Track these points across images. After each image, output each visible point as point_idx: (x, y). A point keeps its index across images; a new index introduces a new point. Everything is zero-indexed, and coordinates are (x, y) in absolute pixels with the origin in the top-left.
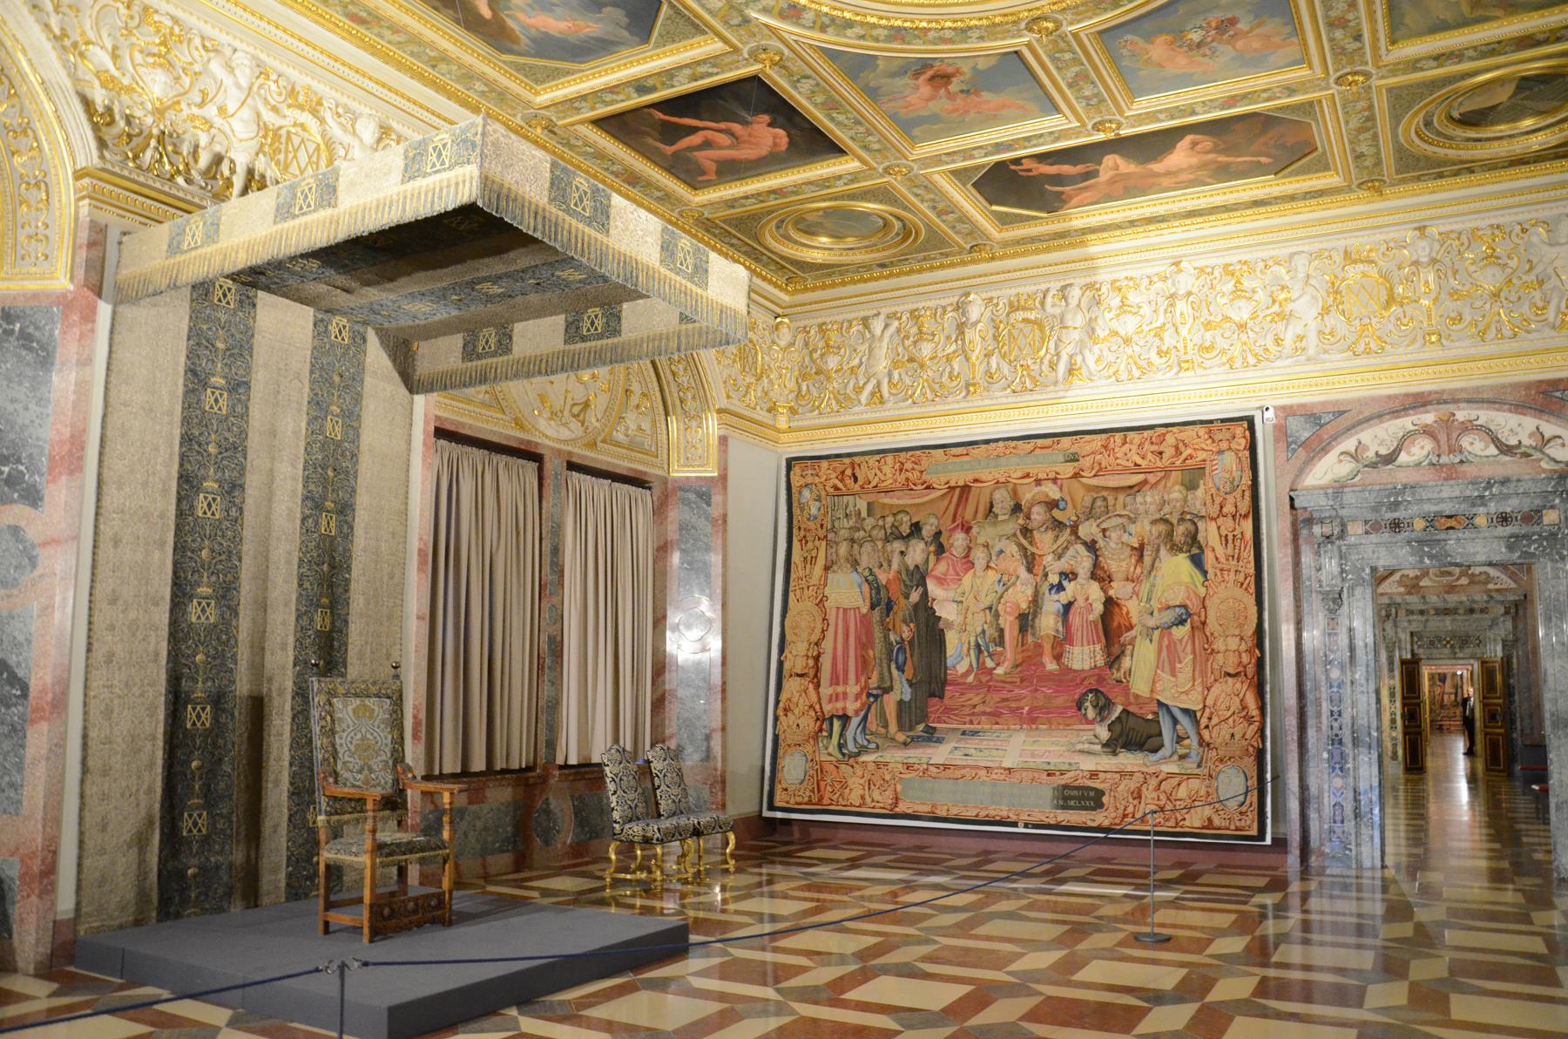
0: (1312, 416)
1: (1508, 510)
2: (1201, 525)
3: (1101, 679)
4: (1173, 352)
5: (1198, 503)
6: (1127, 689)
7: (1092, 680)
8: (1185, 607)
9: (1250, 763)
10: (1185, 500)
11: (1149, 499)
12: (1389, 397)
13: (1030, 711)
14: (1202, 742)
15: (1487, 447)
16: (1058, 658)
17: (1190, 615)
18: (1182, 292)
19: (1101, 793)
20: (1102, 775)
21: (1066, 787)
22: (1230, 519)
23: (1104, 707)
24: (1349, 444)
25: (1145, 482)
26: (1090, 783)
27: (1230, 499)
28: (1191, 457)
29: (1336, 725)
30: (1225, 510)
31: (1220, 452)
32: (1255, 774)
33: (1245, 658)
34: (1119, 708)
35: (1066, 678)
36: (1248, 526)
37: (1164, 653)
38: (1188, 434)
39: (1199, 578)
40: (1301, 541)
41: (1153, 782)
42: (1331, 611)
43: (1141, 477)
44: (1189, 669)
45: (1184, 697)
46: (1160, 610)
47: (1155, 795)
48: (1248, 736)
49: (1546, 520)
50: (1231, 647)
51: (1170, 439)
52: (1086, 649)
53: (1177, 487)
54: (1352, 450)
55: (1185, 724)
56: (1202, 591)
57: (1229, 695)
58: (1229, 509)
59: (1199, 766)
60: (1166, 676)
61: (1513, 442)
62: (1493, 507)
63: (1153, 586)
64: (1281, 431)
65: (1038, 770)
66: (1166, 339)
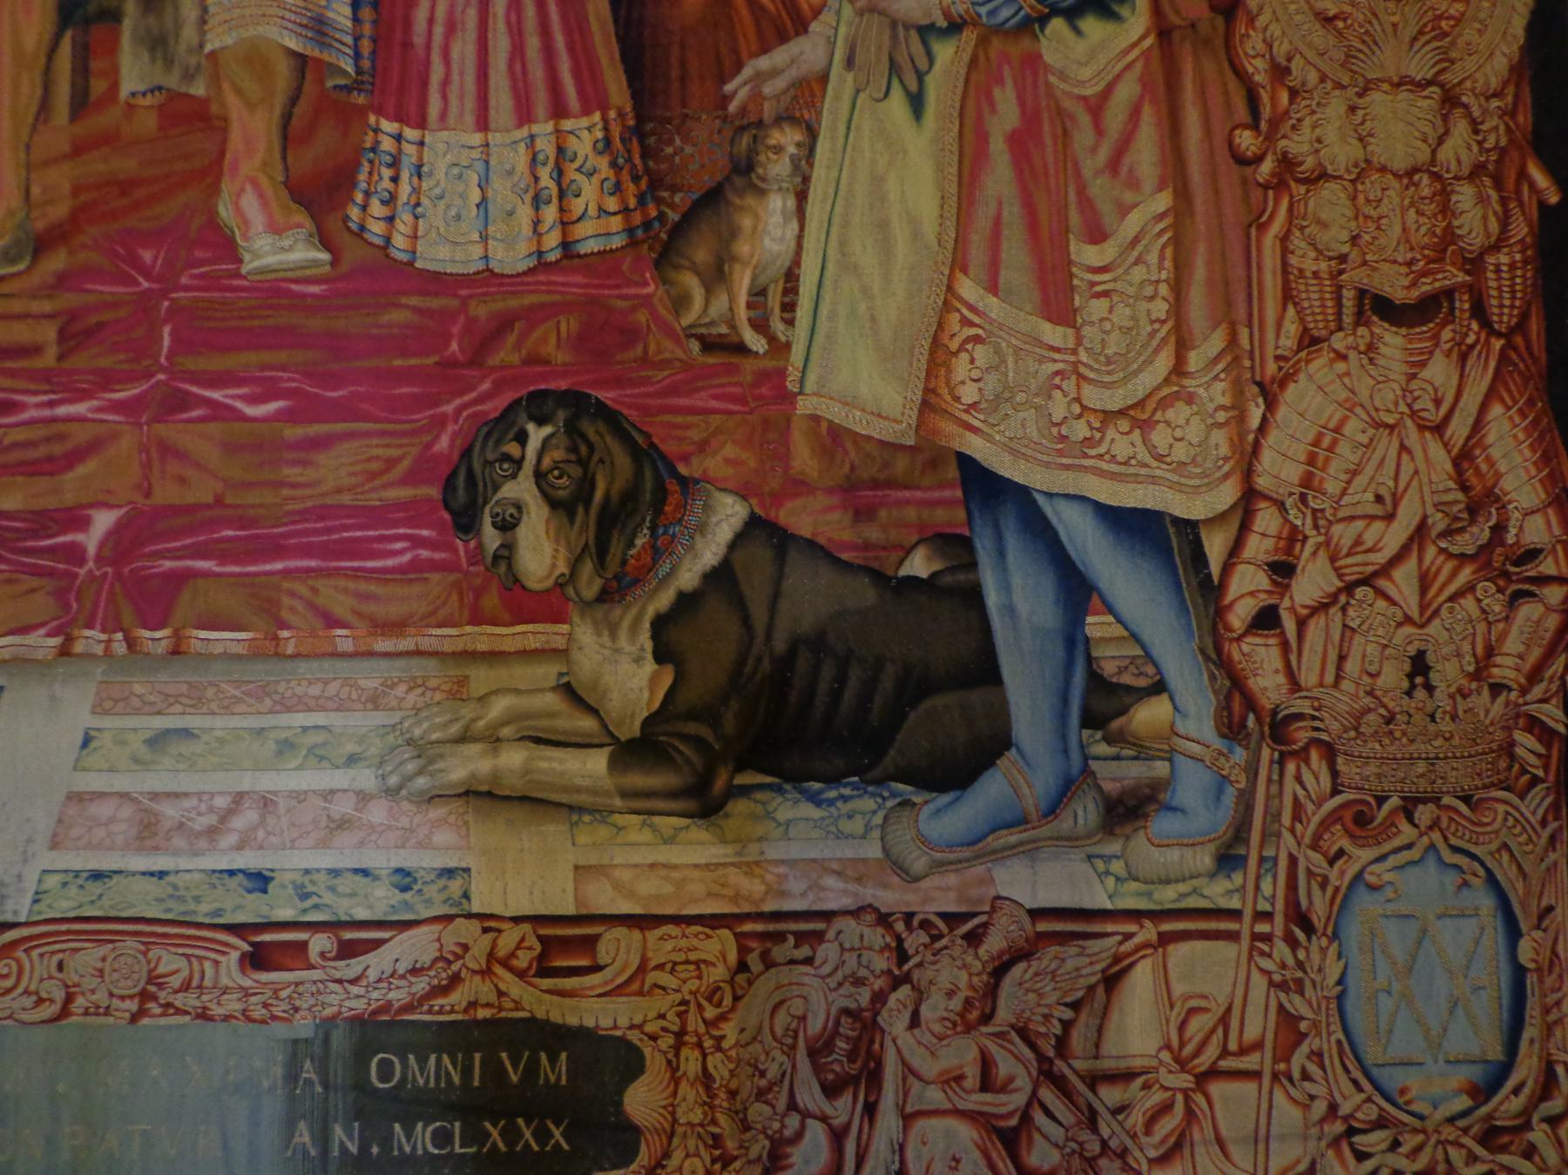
3: (606, 335)
6: (775, 390)
7: (553, 341)
13: (123, 543)
16: (320, 194)
19: (620, 1059)
20: (619, 949)
21: (372, 1031)
23: (621, 508)
26: (533, 1000)
33: (1473, 216)
34: (727, 516)
35: (385, 328)
37: (1000, 178)
41: (951, 975)
44: (1153, 269)
45: (1121, 442)
47: (962, 1054)
48: (1506, 669)
52: (510, 149)
59: (1228, 860)
60: (1009, 312)
65: (183, 930)
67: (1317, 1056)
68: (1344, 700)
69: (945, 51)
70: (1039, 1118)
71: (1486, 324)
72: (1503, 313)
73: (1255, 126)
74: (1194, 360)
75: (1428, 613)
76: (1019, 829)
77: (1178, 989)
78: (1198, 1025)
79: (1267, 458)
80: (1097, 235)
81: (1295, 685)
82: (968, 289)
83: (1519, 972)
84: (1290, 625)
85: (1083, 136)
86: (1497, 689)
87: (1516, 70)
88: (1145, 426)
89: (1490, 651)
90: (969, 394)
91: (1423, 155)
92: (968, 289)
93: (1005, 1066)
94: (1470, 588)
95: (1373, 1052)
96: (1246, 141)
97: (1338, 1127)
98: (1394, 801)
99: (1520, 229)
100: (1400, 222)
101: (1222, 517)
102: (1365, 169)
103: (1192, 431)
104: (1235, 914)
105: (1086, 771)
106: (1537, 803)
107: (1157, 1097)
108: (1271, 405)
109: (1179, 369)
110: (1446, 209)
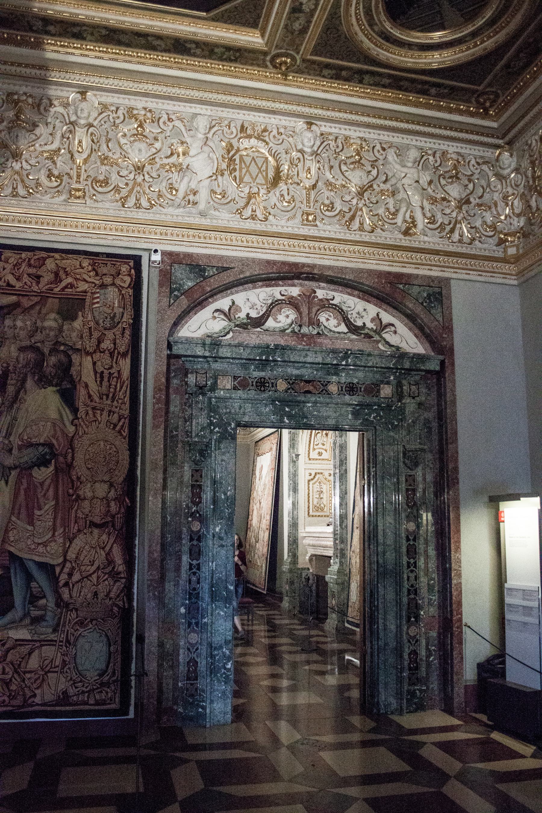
0: (197, 267)
1: (355, 381)
2: (75, 358)
4: (65, 178)
5: (74, 334)
8: (50, 446)
9: (112, 625)
10: (60, 330)
11: (19, 323)
12: (268, 262)
14: (60, 602)
15: (339, 325)
17: (54, 455)
18: (82, 122)
22: (107, 355)
24: (224, 303)
25: (17, 305)
27: (110, 335)
28: (71, 286)
29: (194, 579)
30: (103, 346)
31: (103, 286)
32: (119, 639)
36: (125, 365)
38: (70, 263)
39: (68, 415)
40: (171, 391)
42: (196, 462)
43: (13, 299)
44: (50, 517)
45: (41, 549)
46: (20, 448)
48: (112, 595)
49: (383, 394)
50: (96, 493)
51: (50, 264)
53: (53, 316)
54: (226, 309)
55: (41, 580)
56: (71, 429)
57: (91, 548)
58: (107, 344)
59: (55, 630)
61: (359, 323)
62: (343, 378)
63: (15, 419)
64: (166, 277)
66: (59, 161)
67: (69, 668)
68: (80, 600)
69: (13, 473)
70: (14, 680)
71: (114, 529)
72: (118, 525)
73: (73, 489)
74: (56, 534)
75: (98, 584)
76: (15, 624)
77: (43, 655)
78: (46, 662)
79: (69, 553)
80: (40, 509)
81: (71, 597)
82: (14, 519)
83: (110, 653)
84: (71, 586)
85: (39, 490)
86: (110, 599)
87: (125, 479)
88: (46, 546)
89: (110, 591)
90: (12, 539)
91: (104, 495)
92: (14, 519)
93: (7, 669)
94: (107, 579)
95: (80, 668)
96: (71, 491)
97: (72, 682)
98: (89, 620)
99: (123, 510)
100: (99, 508)
101: (58, 565)
102: (94, 497)
103: (55, 547)
104: (56, 641)
105: (29, 613)
106: (116, 620)
107: (37, 676)
108: (71, 543)
109: (53, 535)
110: (109, 506)
